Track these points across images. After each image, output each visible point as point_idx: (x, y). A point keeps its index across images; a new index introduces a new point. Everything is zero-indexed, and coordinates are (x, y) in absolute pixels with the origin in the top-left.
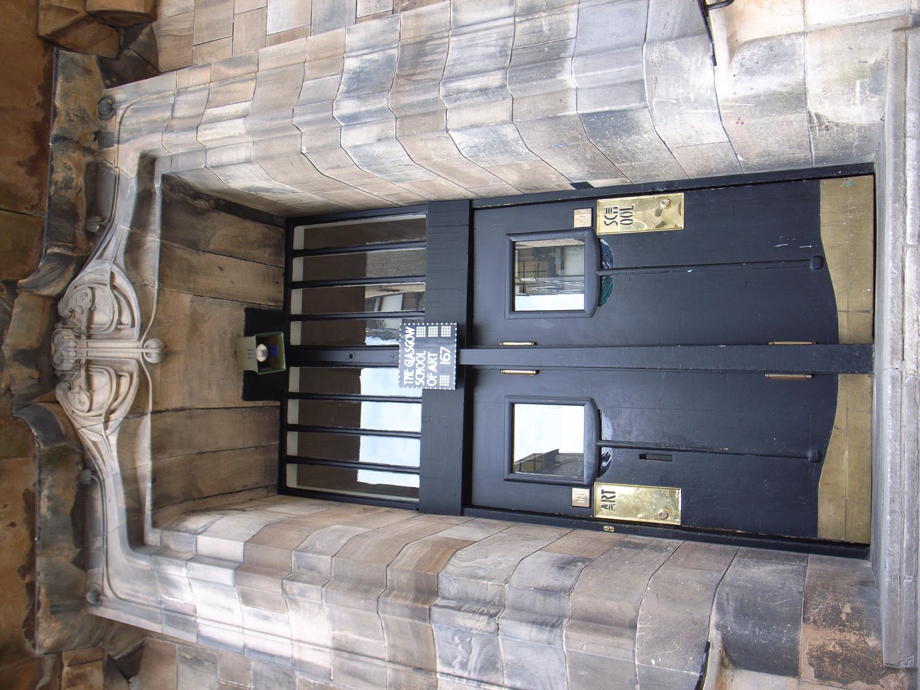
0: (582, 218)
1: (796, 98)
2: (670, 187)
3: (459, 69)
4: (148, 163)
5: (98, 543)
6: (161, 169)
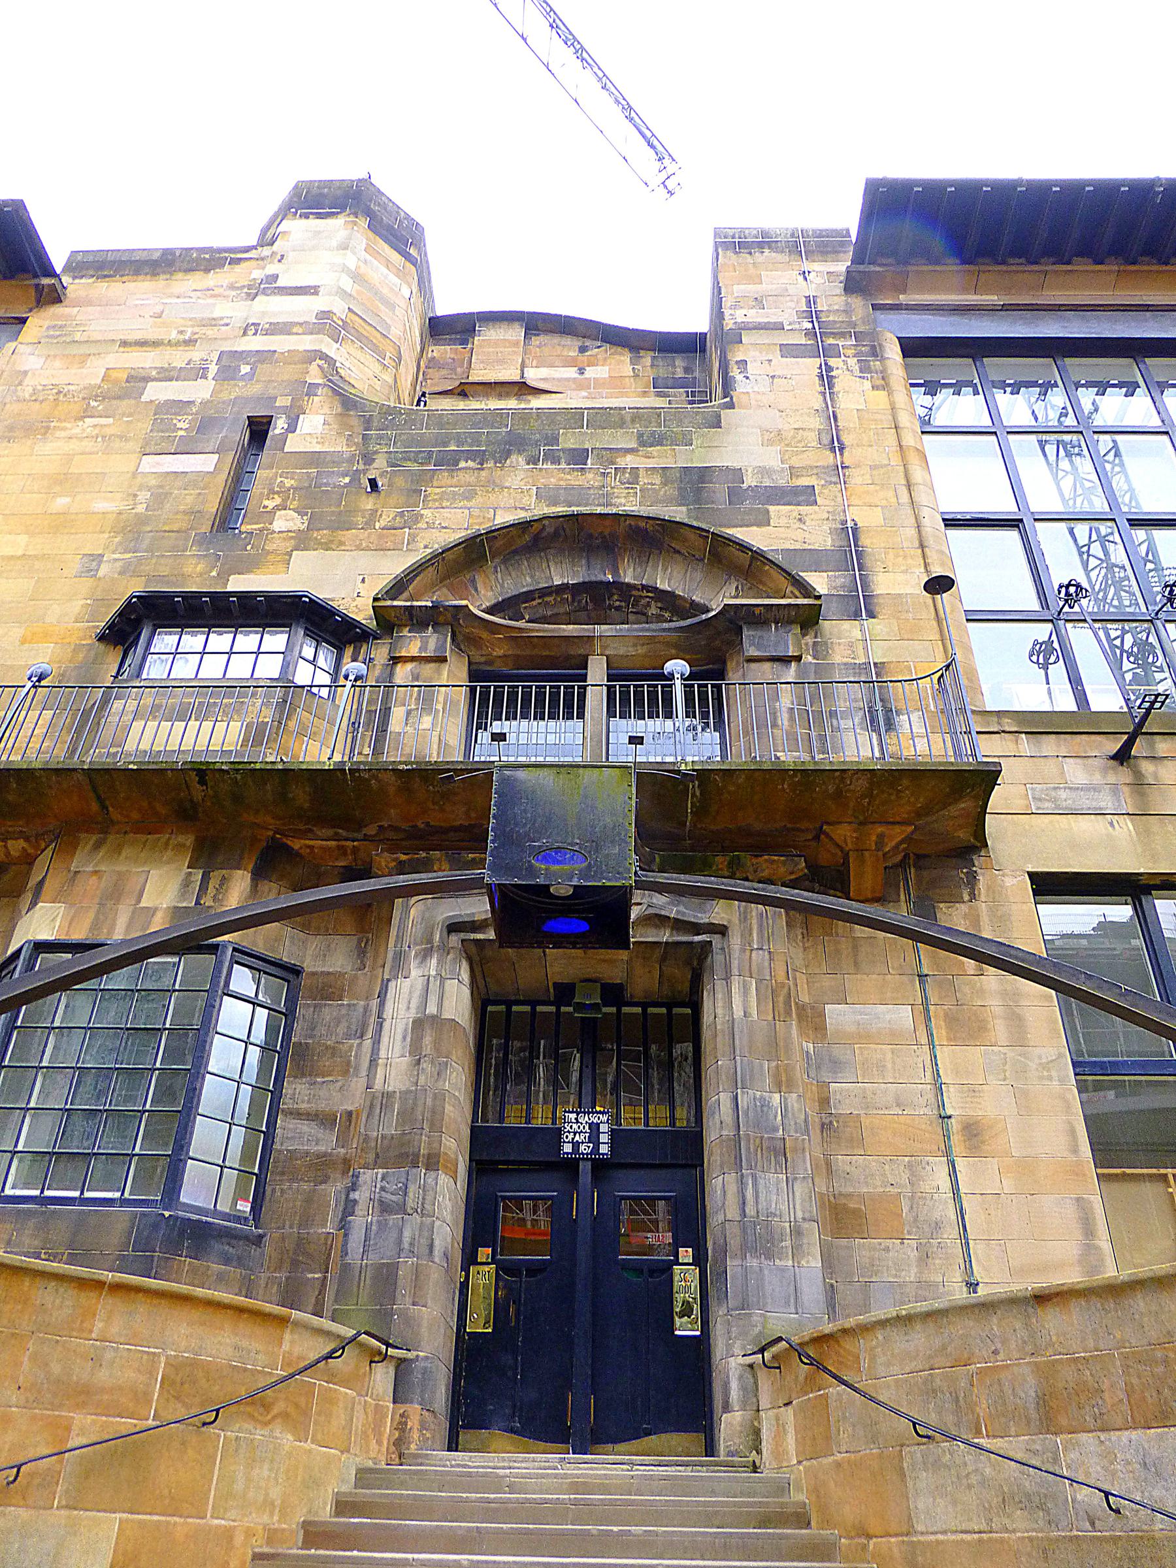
0: (686, 1254)
1: (727, 1408)
3: (762, 1181)
4: (722, 930)
6: (716, 939)
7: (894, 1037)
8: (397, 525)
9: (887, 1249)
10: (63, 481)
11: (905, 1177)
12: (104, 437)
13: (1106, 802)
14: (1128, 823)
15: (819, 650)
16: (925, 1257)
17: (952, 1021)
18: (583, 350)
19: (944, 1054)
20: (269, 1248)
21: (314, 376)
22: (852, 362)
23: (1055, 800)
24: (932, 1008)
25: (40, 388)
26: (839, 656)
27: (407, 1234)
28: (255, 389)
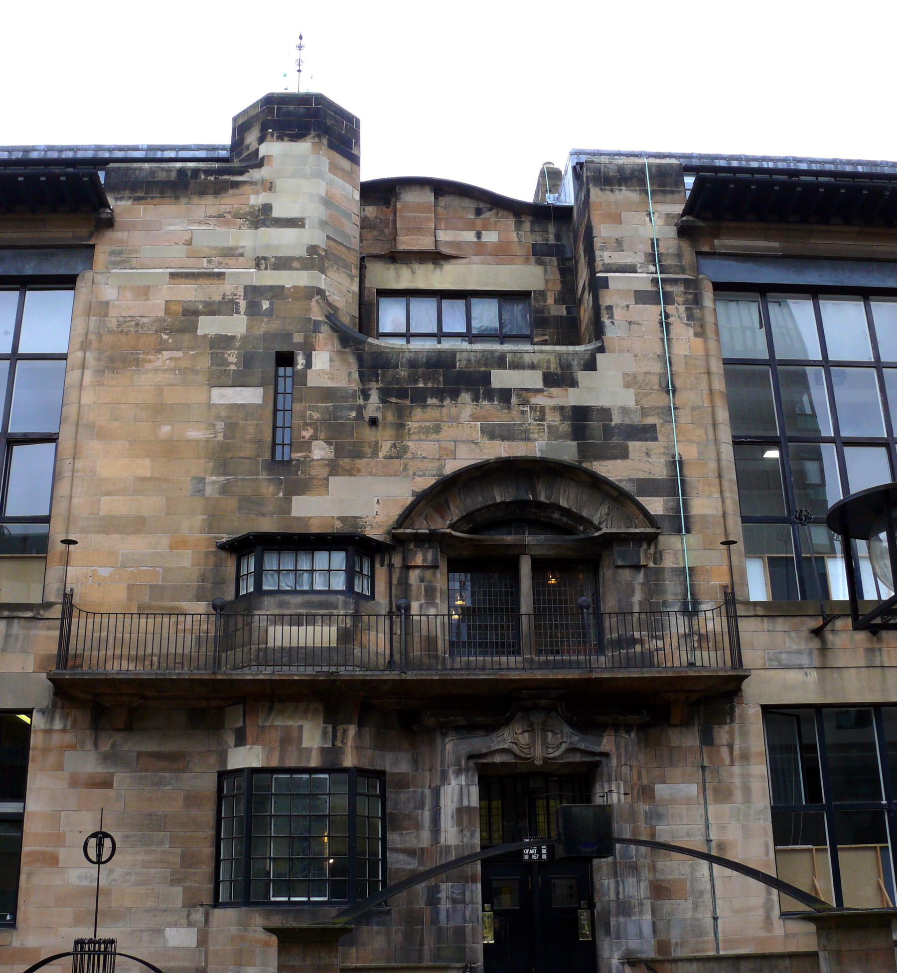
2: (593, 934)
3: (626, 884)
4: (606, 755)
5: (465, 733)
6: (604, 759)
7: (688, 801)
8: (393, 455)
9: (679, 904)
10: (160, 410)
11: (689, 871)
12: (180, 370)
13: (805, 660)
14: (814, 675)
15: (658, 557)
16: (696, 907)
17: (716, 791)
18: (478, 212)
19: (711, 809)
20: (394, 916)
21: (317, 315)
22: (682, 308)
23: (779, 660)
24: (707, 784)
25: (121, 319)
26: (668, 562)
27: (468, 913)
28: (275, 325)
